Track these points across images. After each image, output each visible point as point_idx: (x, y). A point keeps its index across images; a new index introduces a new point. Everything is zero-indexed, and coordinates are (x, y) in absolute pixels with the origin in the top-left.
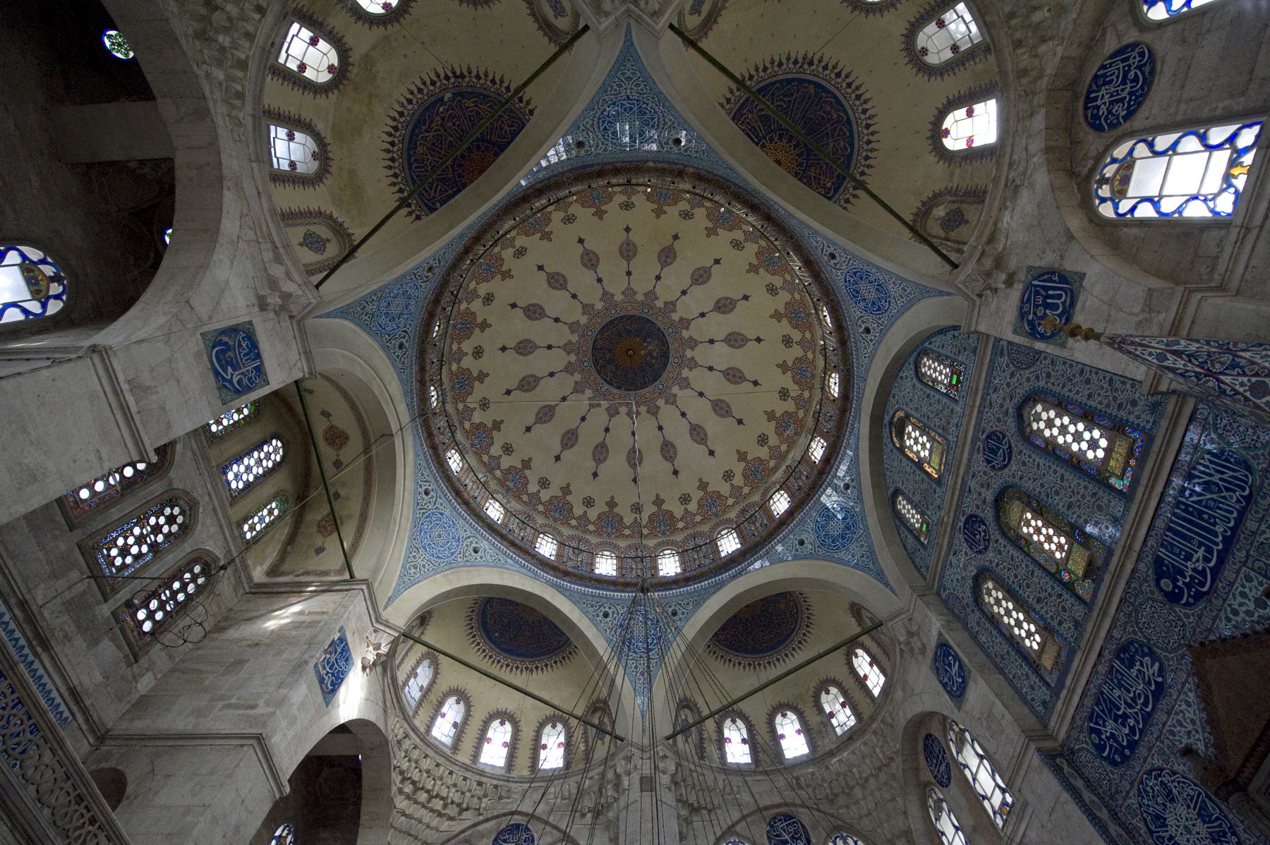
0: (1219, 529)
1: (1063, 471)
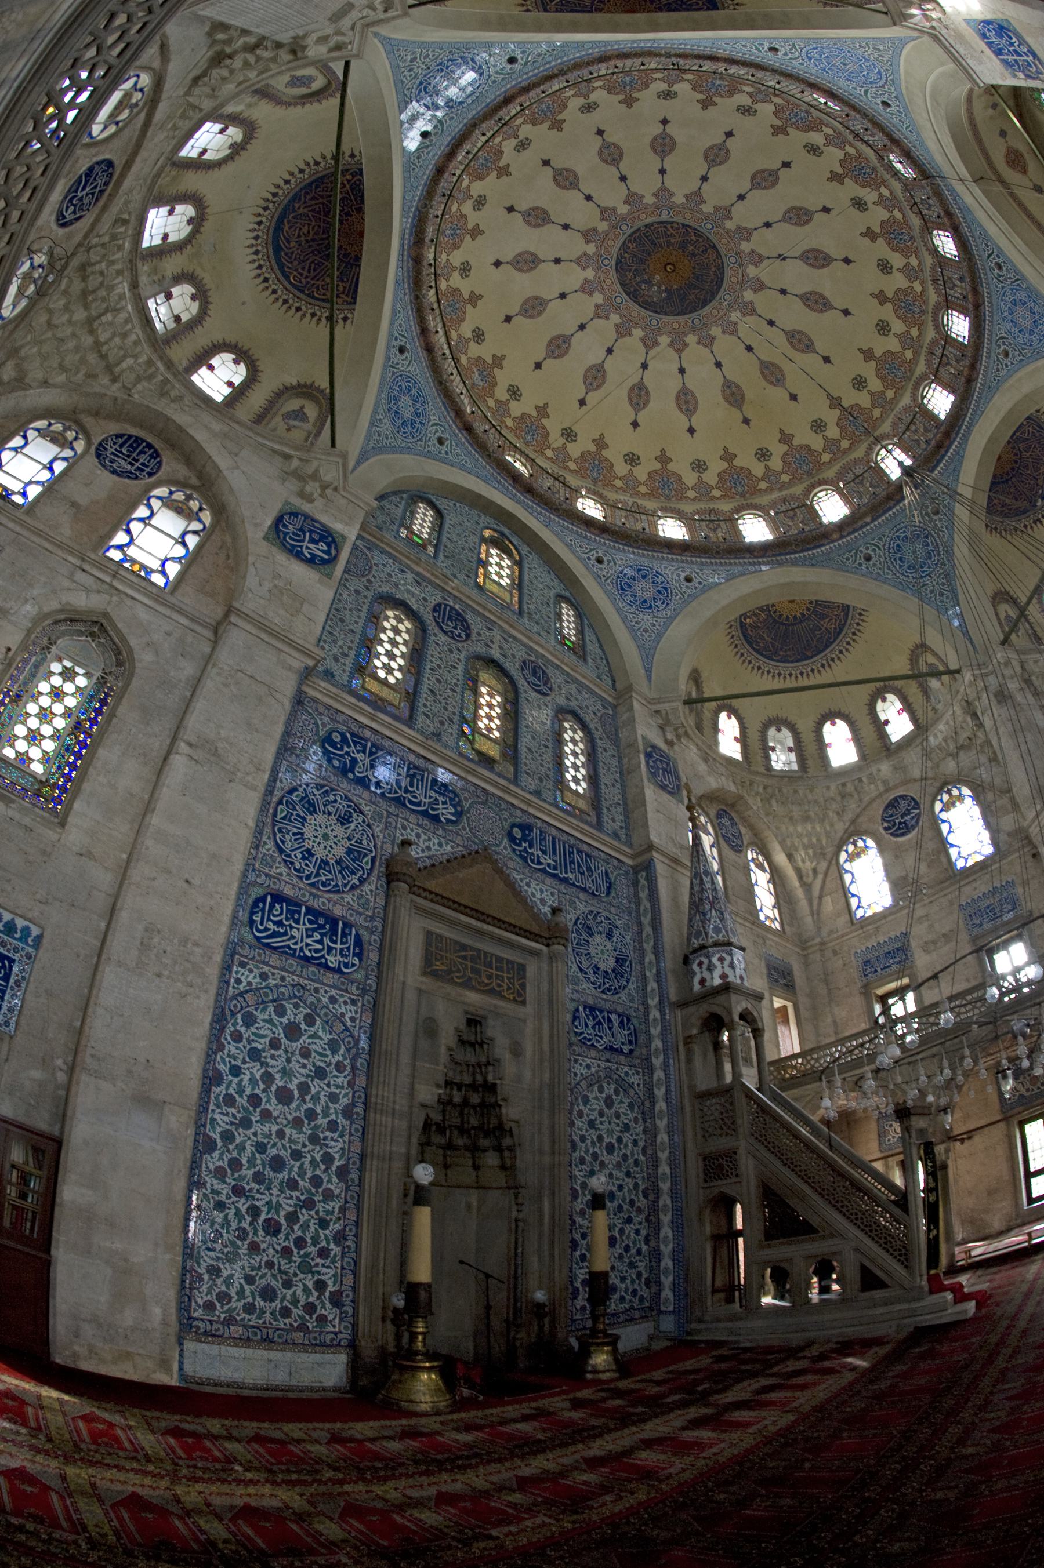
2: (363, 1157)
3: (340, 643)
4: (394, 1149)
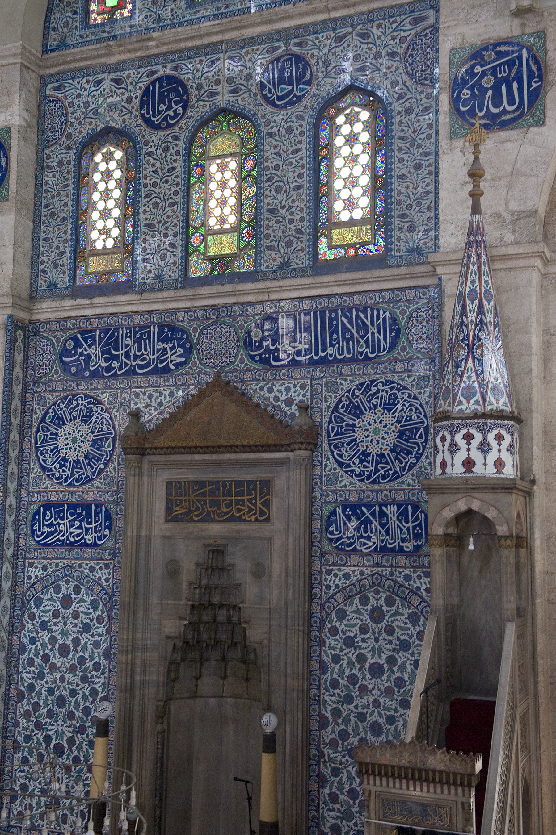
0: (330, 350)
1: (306, 185)
3: (56, 244)
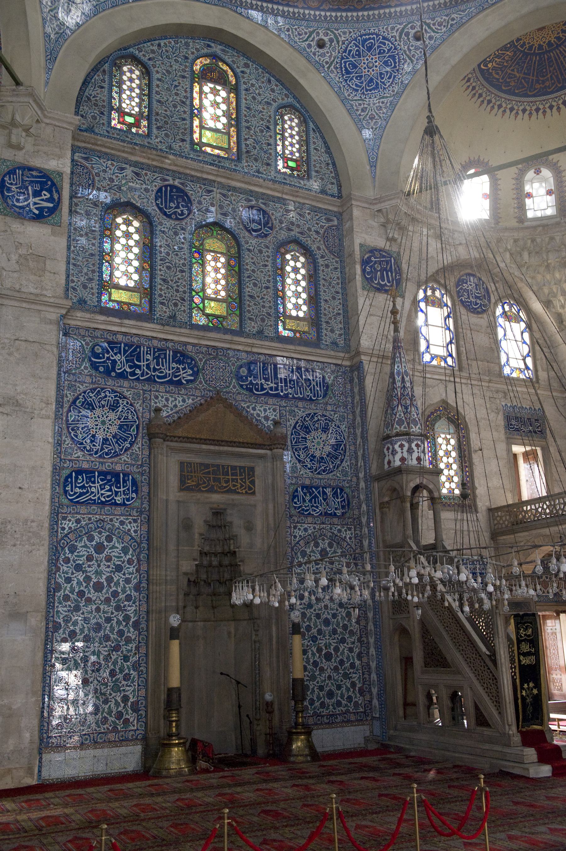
2: (148, 612)
3: (85, 270)
4: (168, 604)
